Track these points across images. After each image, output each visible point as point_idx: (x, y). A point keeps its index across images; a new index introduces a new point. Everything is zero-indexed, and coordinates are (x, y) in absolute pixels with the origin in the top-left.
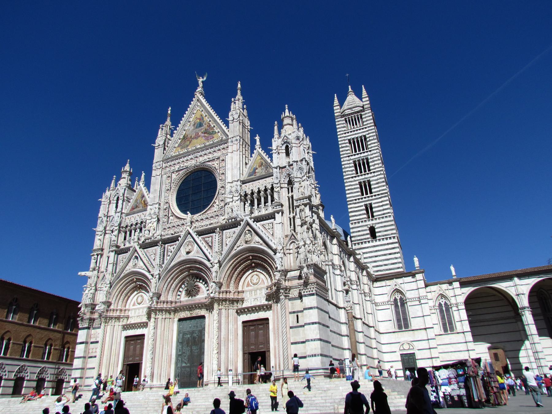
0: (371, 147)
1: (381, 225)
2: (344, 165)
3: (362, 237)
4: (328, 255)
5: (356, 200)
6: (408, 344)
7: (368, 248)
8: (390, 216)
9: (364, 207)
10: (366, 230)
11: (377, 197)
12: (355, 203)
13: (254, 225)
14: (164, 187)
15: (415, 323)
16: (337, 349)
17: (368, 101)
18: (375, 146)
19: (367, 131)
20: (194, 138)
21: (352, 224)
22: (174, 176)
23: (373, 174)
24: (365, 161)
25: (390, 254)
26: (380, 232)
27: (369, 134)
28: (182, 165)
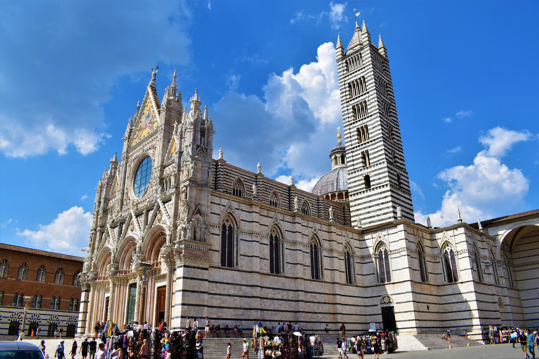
0: (370, 88)
4: (237, 224)
5: (353, 148)
7: (362, 198)
9: (360, 156)
10: (361, 180)
12: (352, 152)
14: (127, 175)
17: (367, 37)
18: (372, 87)
20: (144, 129)
22: (132, 163)
23: (370, 118)
24: (364, 104)
25: (383, 204)
26: (374, 180)
27: (366, 75)
28: (136, 154)
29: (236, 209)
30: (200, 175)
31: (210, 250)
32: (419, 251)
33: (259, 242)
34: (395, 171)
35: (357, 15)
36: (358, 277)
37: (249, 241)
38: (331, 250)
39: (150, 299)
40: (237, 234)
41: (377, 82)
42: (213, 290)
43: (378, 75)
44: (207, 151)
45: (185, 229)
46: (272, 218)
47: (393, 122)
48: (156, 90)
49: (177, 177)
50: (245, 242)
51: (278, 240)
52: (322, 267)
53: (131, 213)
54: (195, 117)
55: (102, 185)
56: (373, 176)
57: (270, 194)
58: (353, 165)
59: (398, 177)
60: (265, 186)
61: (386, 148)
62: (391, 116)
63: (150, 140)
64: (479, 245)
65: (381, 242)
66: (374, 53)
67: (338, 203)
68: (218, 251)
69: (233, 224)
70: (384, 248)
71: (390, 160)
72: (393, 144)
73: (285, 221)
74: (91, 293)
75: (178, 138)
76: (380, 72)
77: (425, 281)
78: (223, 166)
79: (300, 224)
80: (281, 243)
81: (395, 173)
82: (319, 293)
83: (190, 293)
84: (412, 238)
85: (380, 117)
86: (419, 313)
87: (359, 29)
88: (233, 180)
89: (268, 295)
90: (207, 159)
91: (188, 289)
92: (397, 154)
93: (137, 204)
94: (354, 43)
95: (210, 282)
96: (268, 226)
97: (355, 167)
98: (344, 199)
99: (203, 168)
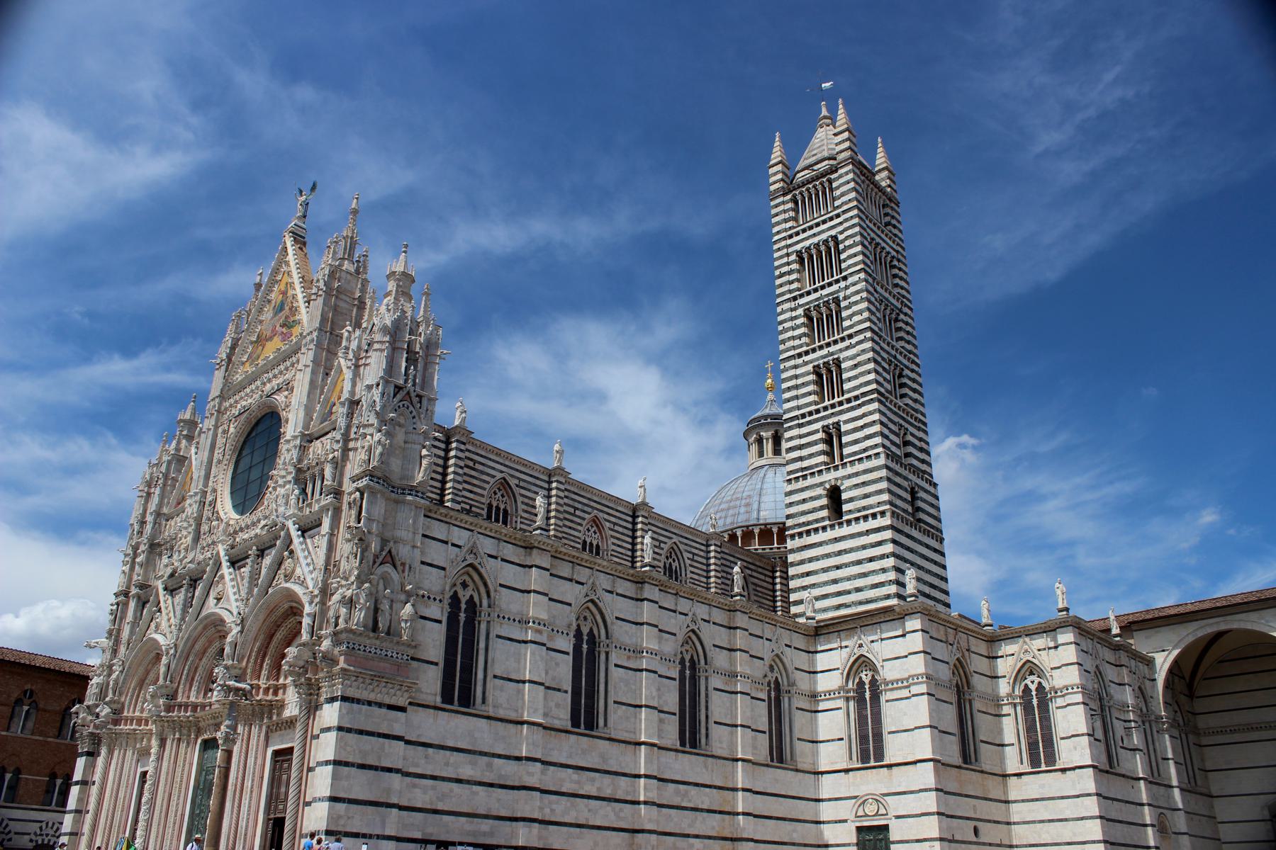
0: (849, 267)
2: (781, 323)
3: (810, 517)
4: (489, 596)
5: (803, 416)
6: (877, 800)
7: (820, 544)
8: (877, 455)
9: (820, 435)
11: (854, 404)
12: (800, 426)
13: (297, 540)
14: (216, 455)
15: (895, 749)
16: (463, 819)
18: (855, 264)
19: (841, 223)
20: (267, 340)
21: (789, 481)
22: (232, 426)
23: (847, 343)
24: (833, 306)
25: (871, 560)
26: (851, 500)
27: (841, 233)
28: (244, 403)
29: (490, 556)
30: (399, 462)
31: (413, 659)
32: (957, 685)
33: (544, 645)
34: (906, 479)
35: (826, 85)
36: (798, 745)
37: (519, 642)
38: (733, 675)
39: (253, 780)
40: (489, 622)
41: (868, 253)
42: (417, 765)
43: (873, 235)
44: (420, 402)
45: (350, 603)
46: (582, 584)
47: (905, 356)
48: (304, 244)
49: (339, 465)
50: (509, 642)
51: (595, 643)
52: (707, 717)
53: (218, 553)
54: (394, 313)
55: (151, 478)
56: (850, 488)
57: (584, 523)
58: (801, 459)
59: (913, 492)
60: (571, 502)
61: (885, 420)
62: (901, 339)
63: (282, 367)
64: (1111, 673)
65: (862, 659)
66: (863, 182)
67: (758, 554)
68: (436, 664)
69: (479, 594)
70: (870, 674)
71: (894, 449)
72: (904, 410)
73: (617, 594)
74: (100, 761)
75: (349, 364)
76: (875, 229)
77: (971, 763)
78: (464, 444)
79: (657, 603)
80: (603, 650)
81: (905, 484)
82: (697, 785)
83: (354, 770)
84: (941, 651)
85: (873, 340)
86: (952, 844)
87: (828, 121)
88: (488, 483)
89: (562, 786)
90: (419, 423)
91: (350, 760)
92: (912, 435)
93: (236, 532)
94: (815, 155)
95: (408, 742)
96: (570, 605)
97: (806, 464)
98: (776, 545)
99: (407, 445)
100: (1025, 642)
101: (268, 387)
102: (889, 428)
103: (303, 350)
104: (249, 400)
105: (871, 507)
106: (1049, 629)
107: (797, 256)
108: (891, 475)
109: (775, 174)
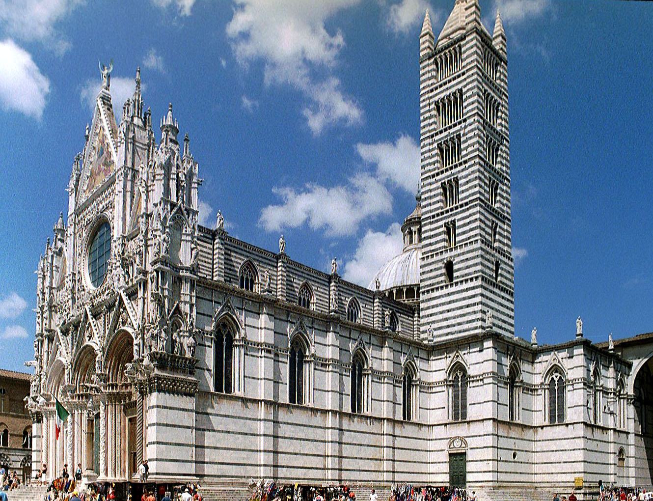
1: (462, 258)
3: (434, 281)
7: (439, 297)
9: (444, 229)
10: (440, 268)
12: (431, 223)
15: (472, 413)
21: (423, 259)
25: (468, 306)
26: (459, 270)
34: (493, 256)
56: (459, 263)
61: (483, 218)
100: (555, 354)
101: (101, 206)
102: (485, 224)
103: (117, 181)
104: (90, 215)
105: (470, 274)
106: (571, 346)
107: (435, 104)
108: (483, 253)
109: (424, 43)
